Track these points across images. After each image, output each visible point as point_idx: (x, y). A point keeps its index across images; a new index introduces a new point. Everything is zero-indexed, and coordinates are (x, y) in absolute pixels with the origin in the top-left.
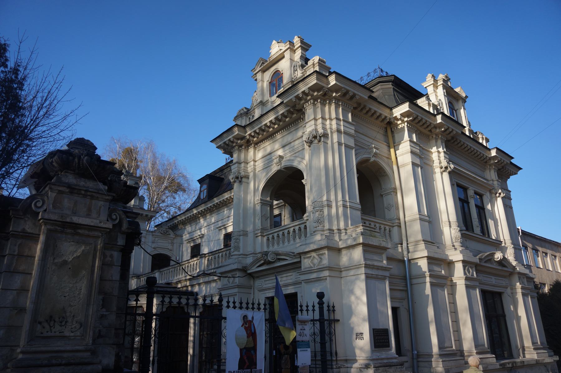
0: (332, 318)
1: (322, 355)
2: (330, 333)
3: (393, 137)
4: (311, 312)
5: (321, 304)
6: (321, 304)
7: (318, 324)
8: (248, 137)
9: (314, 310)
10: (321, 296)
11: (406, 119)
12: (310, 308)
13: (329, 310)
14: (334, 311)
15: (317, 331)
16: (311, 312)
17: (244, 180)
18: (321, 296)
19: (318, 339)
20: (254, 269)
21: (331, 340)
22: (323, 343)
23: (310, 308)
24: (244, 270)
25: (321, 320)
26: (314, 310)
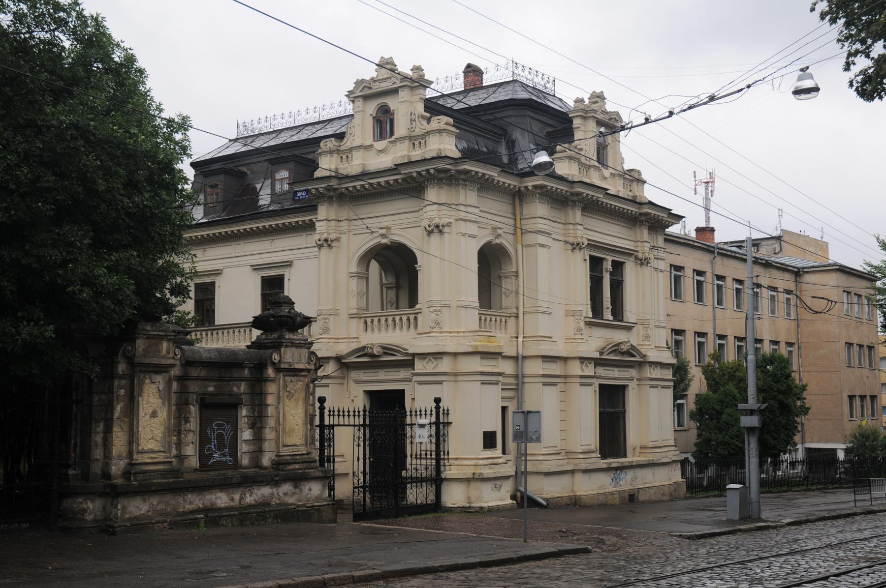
0: (446, 421)
1: (436, 454)
2: (444, 435)
3: (521, 206)
4: (428, 416)
5: (438, 408)
6: (438, 408)
7: (434, 427)
8: (343, 190)
9: (431, 414)
10: (438, 401)
11: (538, 191)
12: (428, 412)
13: (444, 414)
14: (448, 414)
15: (433, 433)
16: (428, 416)
17: (333, 244)
18: (438, 401)
19: (434, 440)
20: (353, 359)
21: (444, 441)
22: (438, 445)
23: (428, 412)
24: (338, 359)
25: (437, 423)
26: (431, 414)
